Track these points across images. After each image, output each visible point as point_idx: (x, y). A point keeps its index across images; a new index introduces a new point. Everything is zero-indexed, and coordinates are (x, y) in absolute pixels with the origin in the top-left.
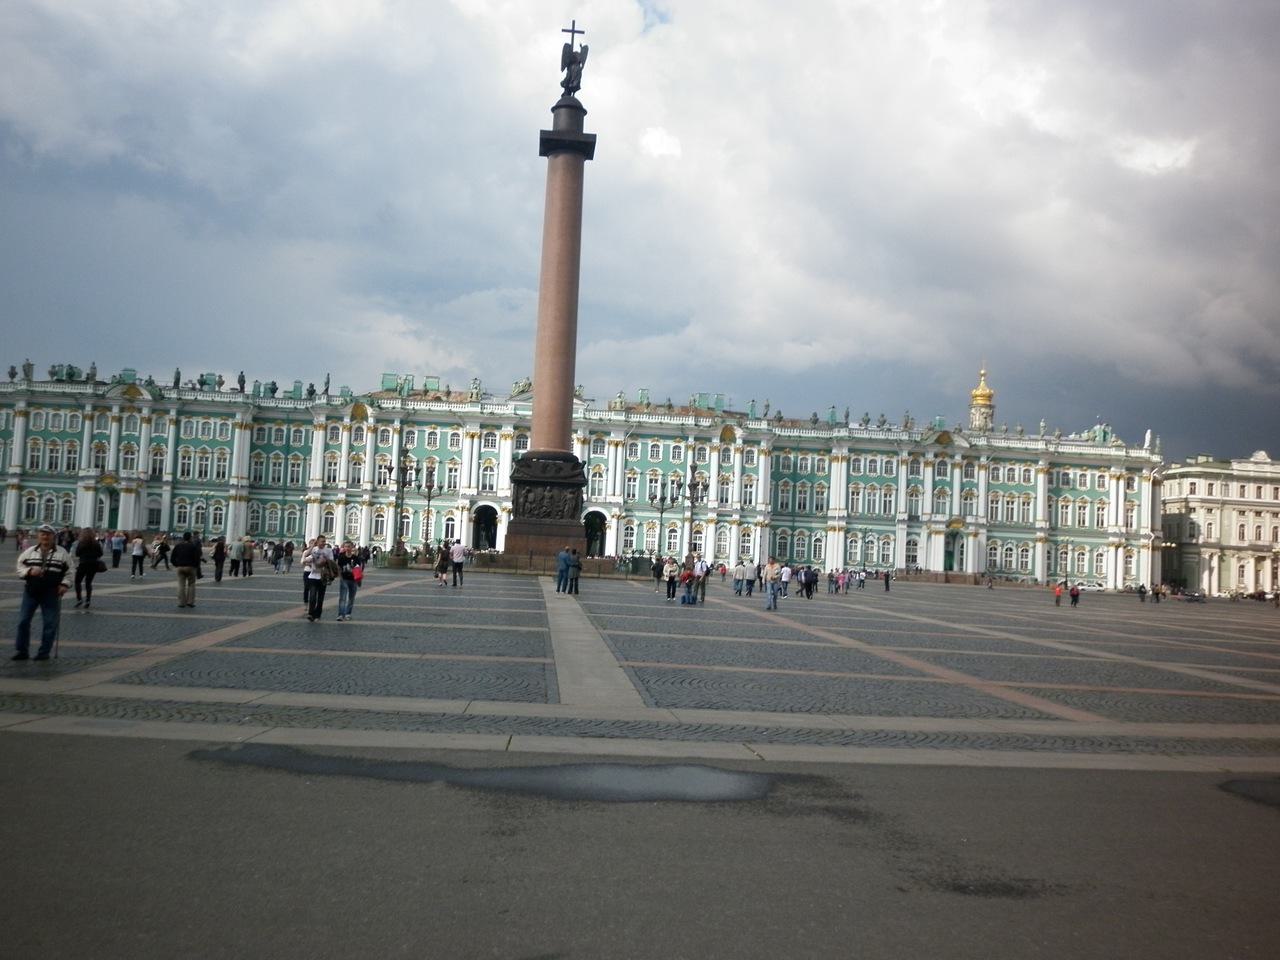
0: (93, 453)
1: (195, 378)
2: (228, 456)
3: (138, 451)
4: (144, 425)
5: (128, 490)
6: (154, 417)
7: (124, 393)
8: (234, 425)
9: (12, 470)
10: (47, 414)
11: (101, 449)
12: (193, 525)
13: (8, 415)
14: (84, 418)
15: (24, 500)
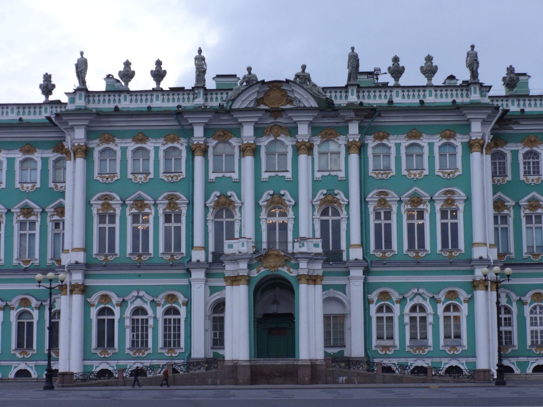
0: (210, 217)
1: (385, 64)
2: (461, 206)
3: (296, 206)
4: (303, 158)
5: (312, 279)
6: (317, 141)
7: (258, 101)
8: (470, 147)
9: (66, 259)
10: (124, 150)
11: (224, 207)
12: (408, 343)
13: (45, 161)
14: (192, 152)
15: (94, 312)
